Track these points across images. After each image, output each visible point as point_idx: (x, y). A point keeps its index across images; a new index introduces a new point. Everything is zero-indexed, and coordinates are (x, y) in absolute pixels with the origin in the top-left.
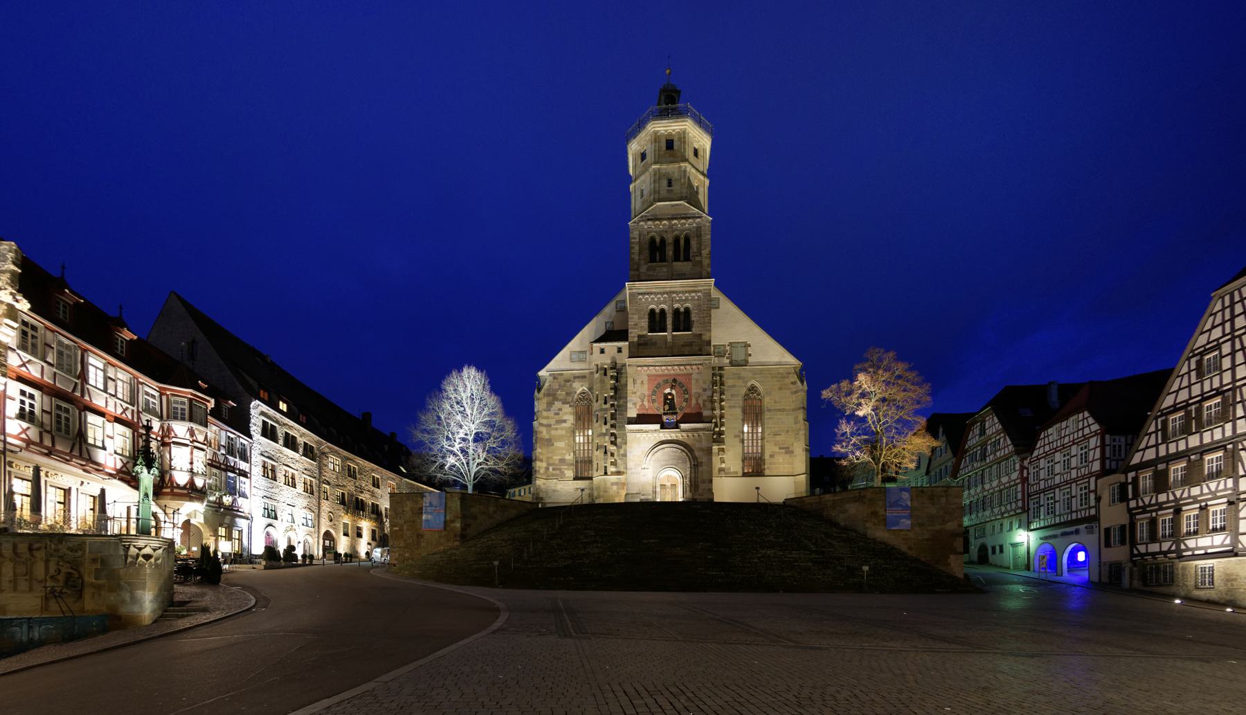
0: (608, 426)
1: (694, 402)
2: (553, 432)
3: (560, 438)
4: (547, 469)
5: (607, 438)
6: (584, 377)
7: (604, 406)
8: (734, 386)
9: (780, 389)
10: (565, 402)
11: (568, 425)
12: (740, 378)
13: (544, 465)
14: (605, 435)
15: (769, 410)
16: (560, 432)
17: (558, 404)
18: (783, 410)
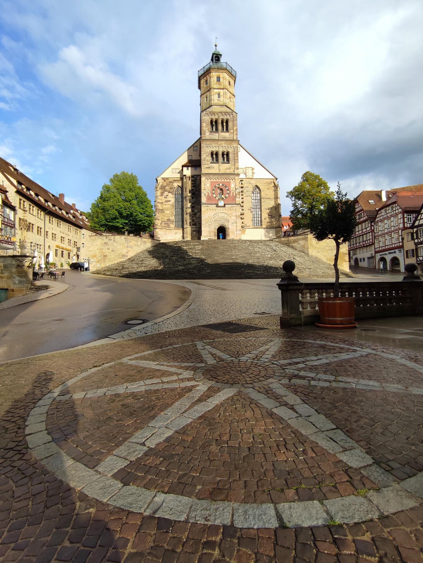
1: (231, 194)
2: (164, 206)
3: (167, 209)
4: (161, 224)
8: (247, 187)
10: (169, 192)
11: (171, 203)
12: (250, 183)
13: (160, 222)
15: (264, 198)
17: (166, 193)
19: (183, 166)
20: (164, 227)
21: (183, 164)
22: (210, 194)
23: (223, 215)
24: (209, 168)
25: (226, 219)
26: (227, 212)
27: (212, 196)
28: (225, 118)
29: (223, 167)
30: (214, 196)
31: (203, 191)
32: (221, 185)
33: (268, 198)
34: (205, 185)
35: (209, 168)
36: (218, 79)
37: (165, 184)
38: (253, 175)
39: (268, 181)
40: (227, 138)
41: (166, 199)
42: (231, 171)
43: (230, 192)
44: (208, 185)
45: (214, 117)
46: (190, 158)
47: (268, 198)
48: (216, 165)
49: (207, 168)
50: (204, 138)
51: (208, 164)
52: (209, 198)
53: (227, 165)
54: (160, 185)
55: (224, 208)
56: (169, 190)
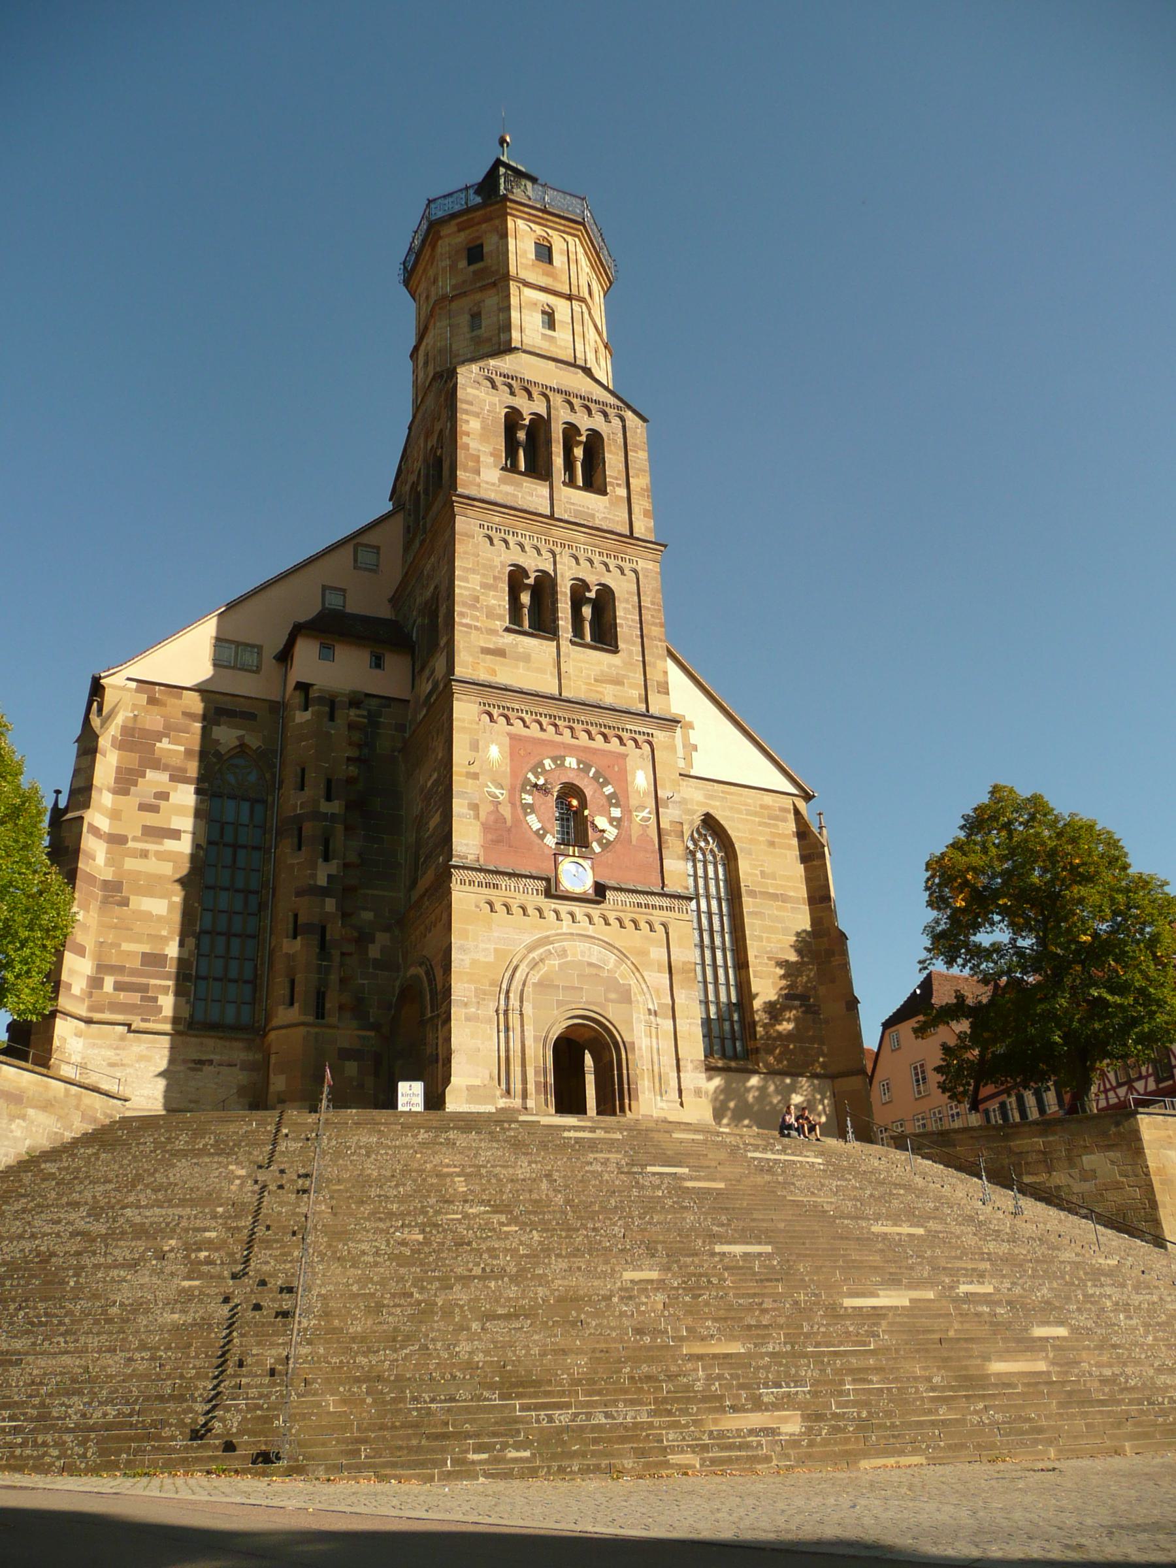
0: (333, 867)
2: (130, 864)
3: (151, 887)
4: (96, 983)
5: (330, 905)
6: (252, 716)
7: (326, 807)
9: (772, 844)
14: (324, 892)
15: (752, 894)
16: (152, 866)
17: (156, 779)
18: (784, 898)
19: (298, 631)
20: (115, 1007)
21: (303, 618)
22: (506, 811)
23: (596, 953)
24: (500, 653)
25: (612, 984)
26: (611, 933)
27: (518, 823)
28: (585, 423)
29: (585, 670)
30: (534, 822)
31: (460, 783)
32: (571, 762)
33: (775, 897)
34: (475, 746)
35: (500, 653)
36: (545, 253)
37: (154, 720)
38: (688, 759)
39: (768, 799)
40: (597, 523)
41: (150, 819)
42: (630, 696)
43: (627, 811)
44: (495, 753)
45: (529, 408)
46: (334, 601)
47: (775, 897)
48: (538, 648)
49: (486, 651)
50: (472, 492)
51: (493, 632)
52: (499, 832)
53: (599, 659)
54: (119, 720)
55: (595, 911)
56: (176, 761)
